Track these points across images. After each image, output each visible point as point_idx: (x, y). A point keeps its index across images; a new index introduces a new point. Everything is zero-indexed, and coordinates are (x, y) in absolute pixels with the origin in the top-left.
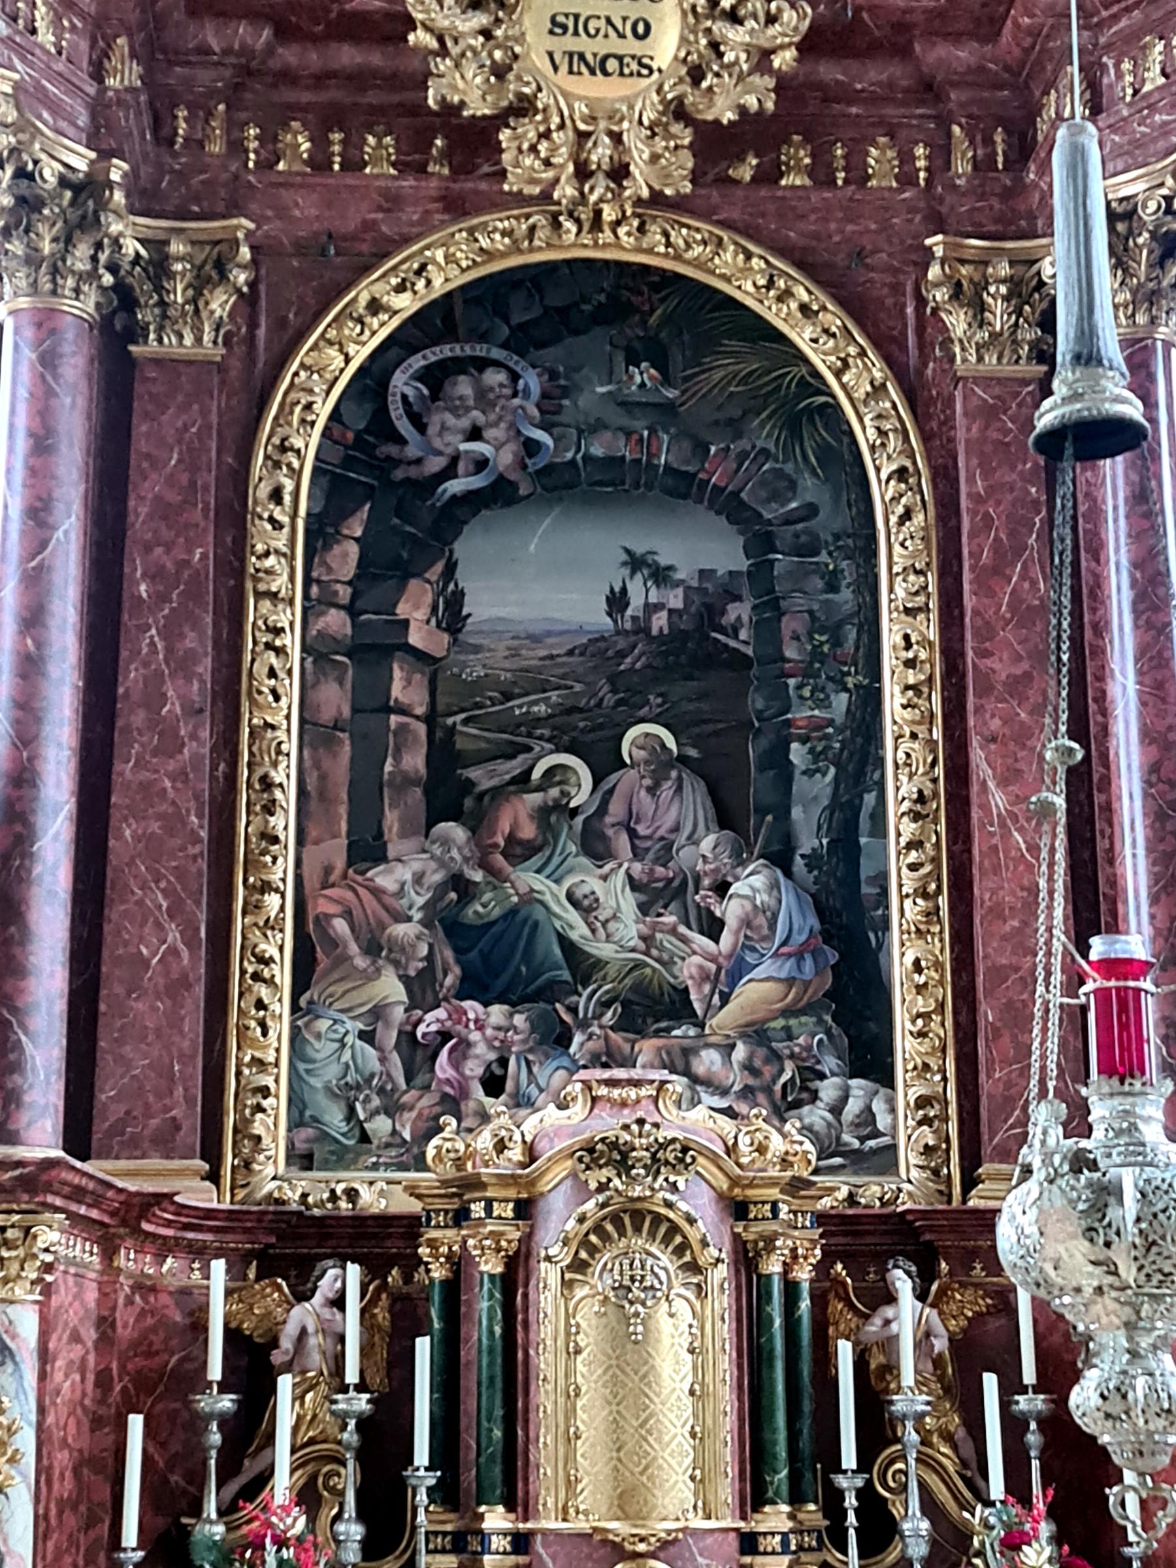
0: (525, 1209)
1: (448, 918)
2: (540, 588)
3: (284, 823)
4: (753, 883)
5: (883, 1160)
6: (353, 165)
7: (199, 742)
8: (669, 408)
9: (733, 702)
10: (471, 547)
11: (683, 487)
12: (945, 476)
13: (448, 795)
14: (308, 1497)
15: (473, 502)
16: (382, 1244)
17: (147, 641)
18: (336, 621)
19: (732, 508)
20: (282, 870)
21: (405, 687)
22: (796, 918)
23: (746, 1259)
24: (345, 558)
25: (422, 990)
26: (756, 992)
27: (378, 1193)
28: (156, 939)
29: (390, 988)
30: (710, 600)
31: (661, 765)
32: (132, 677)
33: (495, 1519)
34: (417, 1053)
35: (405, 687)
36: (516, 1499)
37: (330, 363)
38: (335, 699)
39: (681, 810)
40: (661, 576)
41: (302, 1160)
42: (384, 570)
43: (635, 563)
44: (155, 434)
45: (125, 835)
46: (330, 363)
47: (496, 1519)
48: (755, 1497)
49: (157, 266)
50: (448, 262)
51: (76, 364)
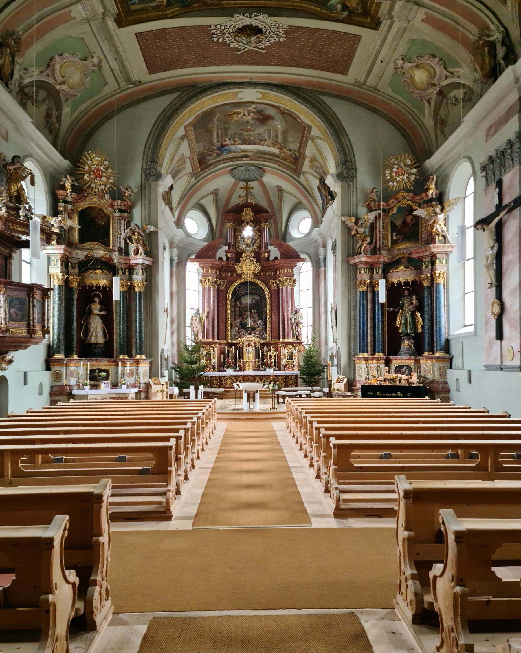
0: (243, 344)
1: (241, 324)
2: (247, 300)
3: (230, 319)
4: (260, 321)
5: (266, 339)
6: (233, 275)
7: (224, 314)
8: (255, 289)
9: (259, 307)
10: (242, 298)
11: (256, 294)
12: (271, 295)
13: (241, 316)
14: (232, 359)
15: (242, 296)
16: (235, 345)
17: (221, 308)
18: (233, 304)
19: (259, 296)
20: (230, 322)
21: (237, 309)
22: (262, 323)
23: (255, 346)
24: (233, 300)
25: (239, 329)
26: (260, 328)
27: (236, 342)
28: (222, 327)
29: (237, 328)
30: (258, 301)
31: (255, 312)
32: (220, 310)
33: (241, 360)
34: (239, 333)
35: (237, 309)
36: (243, 359)
37: (232, 289)
38: (233, 309)
39: (256, 316)
40: (255, 299)
41: (231, 339)
42: (236, 301)
43: (253, 298)
44: (221, 294)
45: (220, 320)
46: (232, 289)
47: (241, 360)
48: (256, 359)
49: (220, 283)
50: (239, 282)
51: (216, 292)
